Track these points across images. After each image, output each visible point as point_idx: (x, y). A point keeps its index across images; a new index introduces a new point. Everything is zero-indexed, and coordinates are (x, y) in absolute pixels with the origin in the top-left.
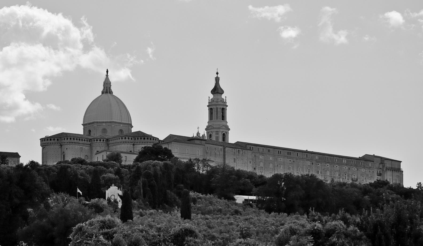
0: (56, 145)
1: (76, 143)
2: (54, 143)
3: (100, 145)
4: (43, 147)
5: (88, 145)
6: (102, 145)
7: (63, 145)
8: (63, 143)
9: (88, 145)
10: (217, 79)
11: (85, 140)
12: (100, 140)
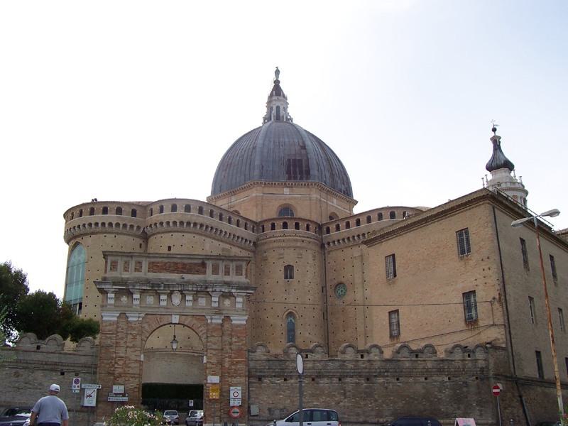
0: (124, 234)
2: (118, 225)
3: (299, 244)
4: (73, 242)
6: (304, 245)
7: (154, 234)
10: (496, 142)
11: (238, 221)
12: (297, 226)
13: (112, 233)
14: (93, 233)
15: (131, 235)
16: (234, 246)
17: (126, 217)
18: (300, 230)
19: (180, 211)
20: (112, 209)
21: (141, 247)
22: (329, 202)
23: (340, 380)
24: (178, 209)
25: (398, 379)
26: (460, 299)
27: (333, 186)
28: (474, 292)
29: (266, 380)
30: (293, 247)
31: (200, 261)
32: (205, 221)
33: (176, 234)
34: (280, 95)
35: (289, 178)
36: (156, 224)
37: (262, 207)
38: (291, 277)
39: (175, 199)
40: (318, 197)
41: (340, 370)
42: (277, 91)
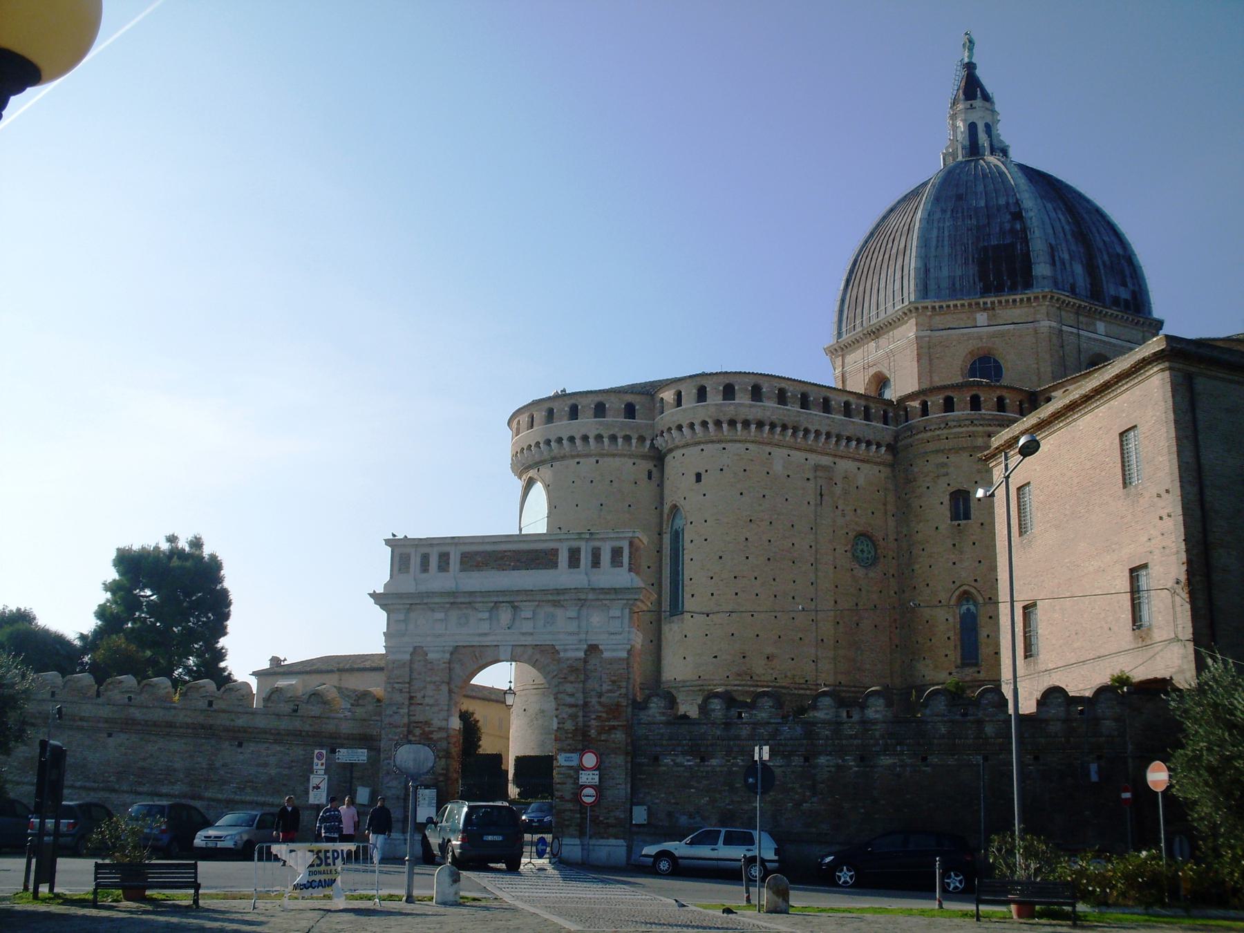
0: (614, 455)
1: (773, 426)
2: (599, 438)
5: (879, 445)
7: (671, 451)
8: (669, 429)
9: (879, 445)
12: (975, 404)
13: (587, 456)
14: (554, 459)
15: (630, 456)
16: (842, 457)
17: (615, 420)
18: (983, 412)
19: (715, 398)
20: (587, 405)
21: (650, 478)
22: (1081, 332)
23: (806, 759)
24: (709, 395)
25: (924, 759)
26: (1124, 584)
27: (1096, 293)
28: (1145, 566)
29: (668, 761)
30: (963, 449)
31: (594, 537)
32: (768, 413)
33: (710, 445)
34: (974, 98)
35: (986, 291)
36: (669, 429)
37: (930, 360)
38: (967, 516)
39: (703, 375)
40: (1054, 324)
41: (805, 742)
42: (972, 88)
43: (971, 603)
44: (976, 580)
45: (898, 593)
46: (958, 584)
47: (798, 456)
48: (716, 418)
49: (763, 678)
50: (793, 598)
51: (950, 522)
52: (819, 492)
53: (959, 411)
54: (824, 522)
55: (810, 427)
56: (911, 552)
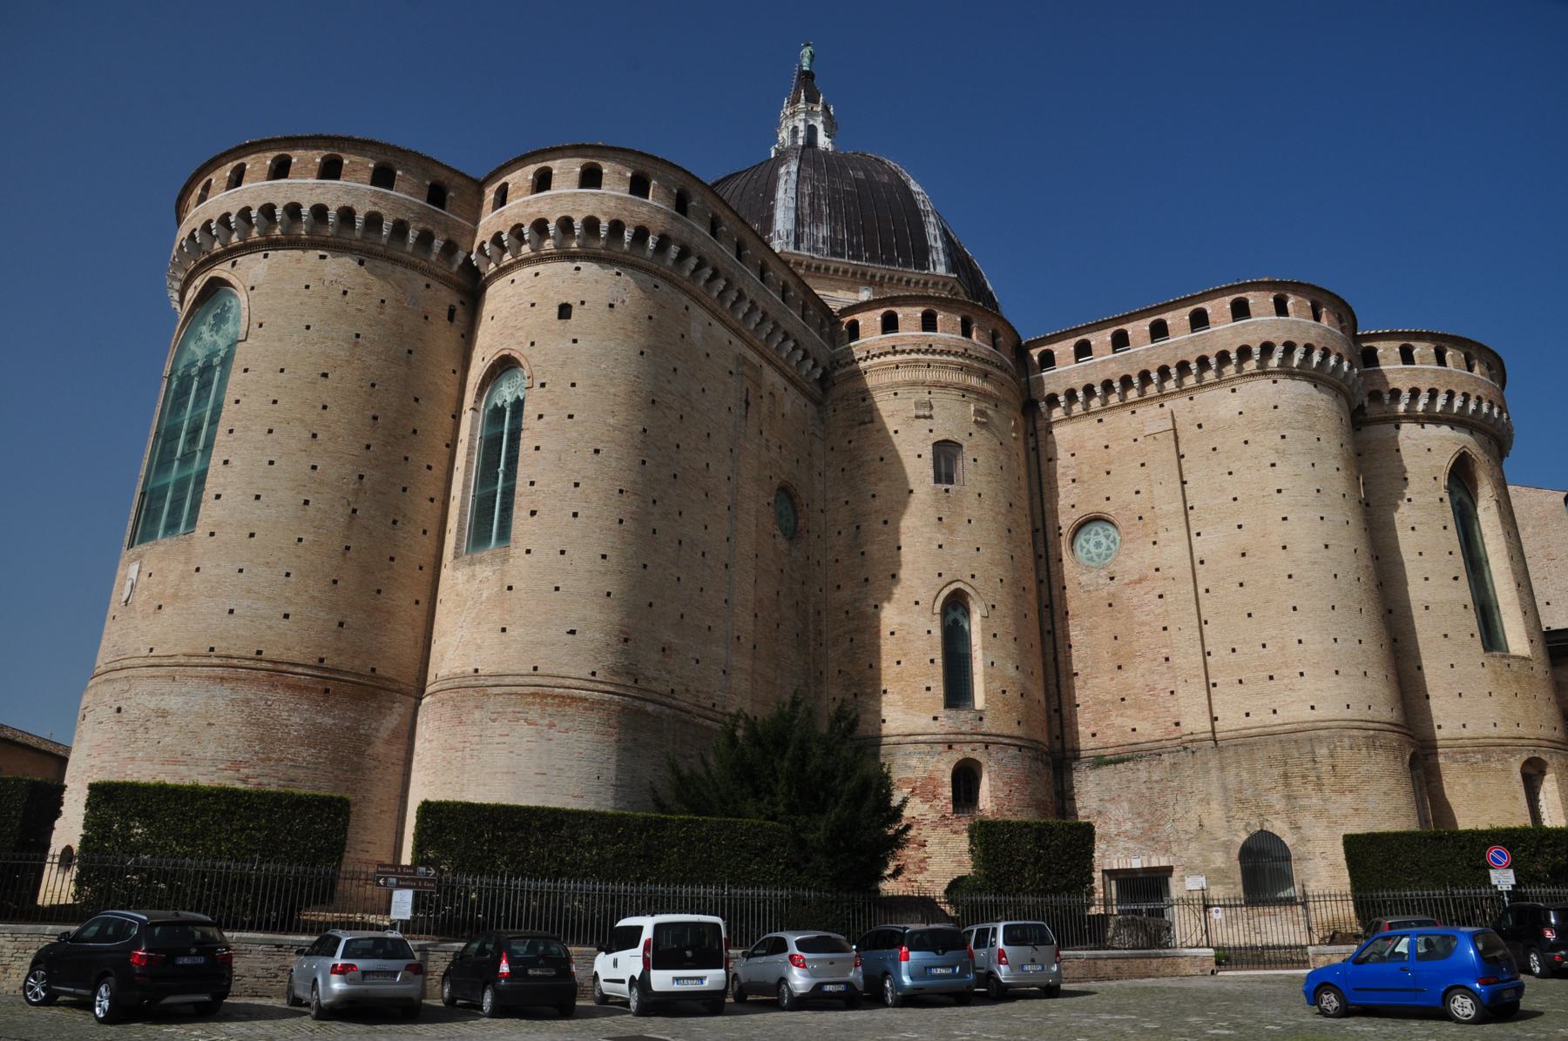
2: (374, 220)
15: (423, 272)
21: (451, 317)
43: (960, 610)
44: (973, 576)
45: (824, 590)
46: (946, 578)
47: (720, 331)
48: (614, 218)
49: (655, 686)
50: (703, 554)
51: (932, 484)
52: (744, 398)
53: (945, 332)
54: (748, 446)
55: (746, 292)
56: (858, 527)
